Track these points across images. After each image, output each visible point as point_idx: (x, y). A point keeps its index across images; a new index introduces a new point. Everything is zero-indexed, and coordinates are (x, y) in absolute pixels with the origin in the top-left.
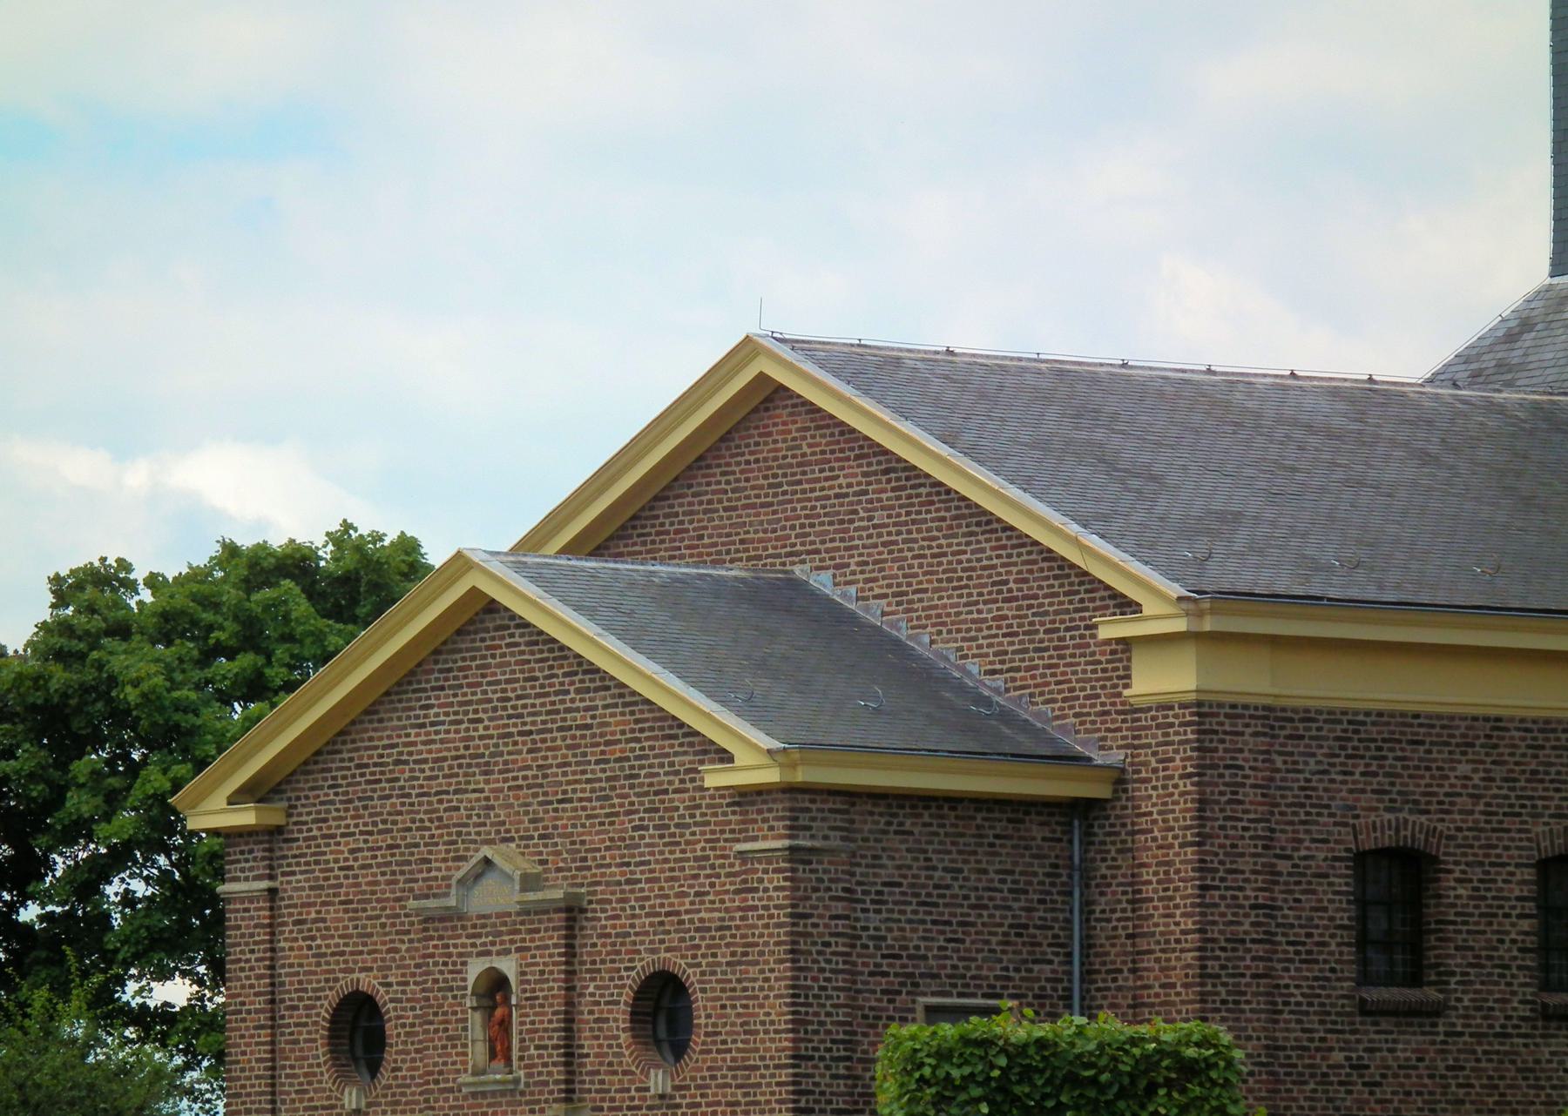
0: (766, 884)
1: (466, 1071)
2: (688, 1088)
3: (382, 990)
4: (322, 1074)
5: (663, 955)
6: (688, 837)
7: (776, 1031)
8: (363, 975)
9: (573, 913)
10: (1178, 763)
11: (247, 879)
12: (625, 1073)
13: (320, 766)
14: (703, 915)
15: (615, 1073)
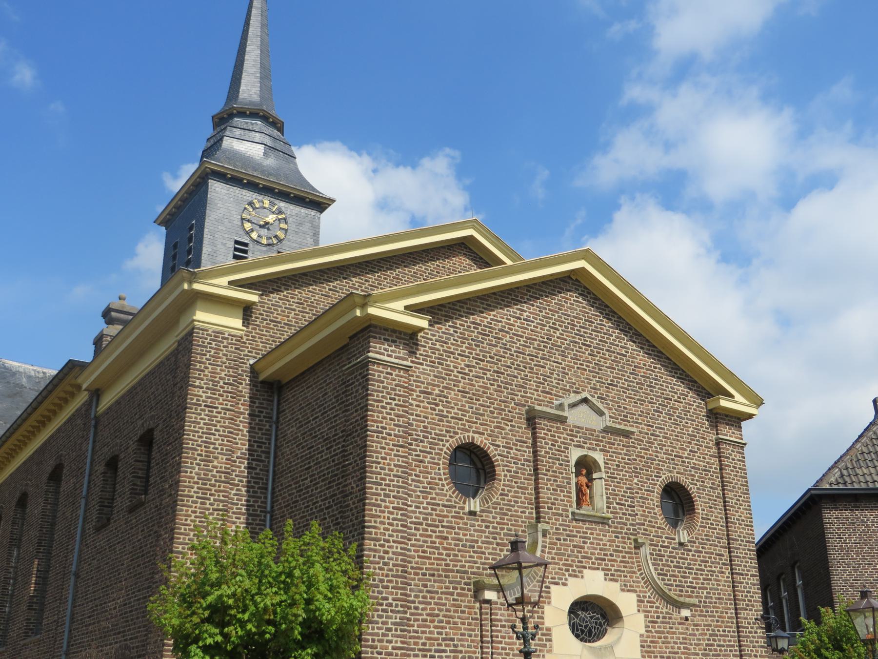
2: (695, 542)
3: (492, 448)
4: (443, 485)
7: (745, 525)
8: (476, 436)
12: (659, 528)
13: (443, 313)
15: (654, 527)
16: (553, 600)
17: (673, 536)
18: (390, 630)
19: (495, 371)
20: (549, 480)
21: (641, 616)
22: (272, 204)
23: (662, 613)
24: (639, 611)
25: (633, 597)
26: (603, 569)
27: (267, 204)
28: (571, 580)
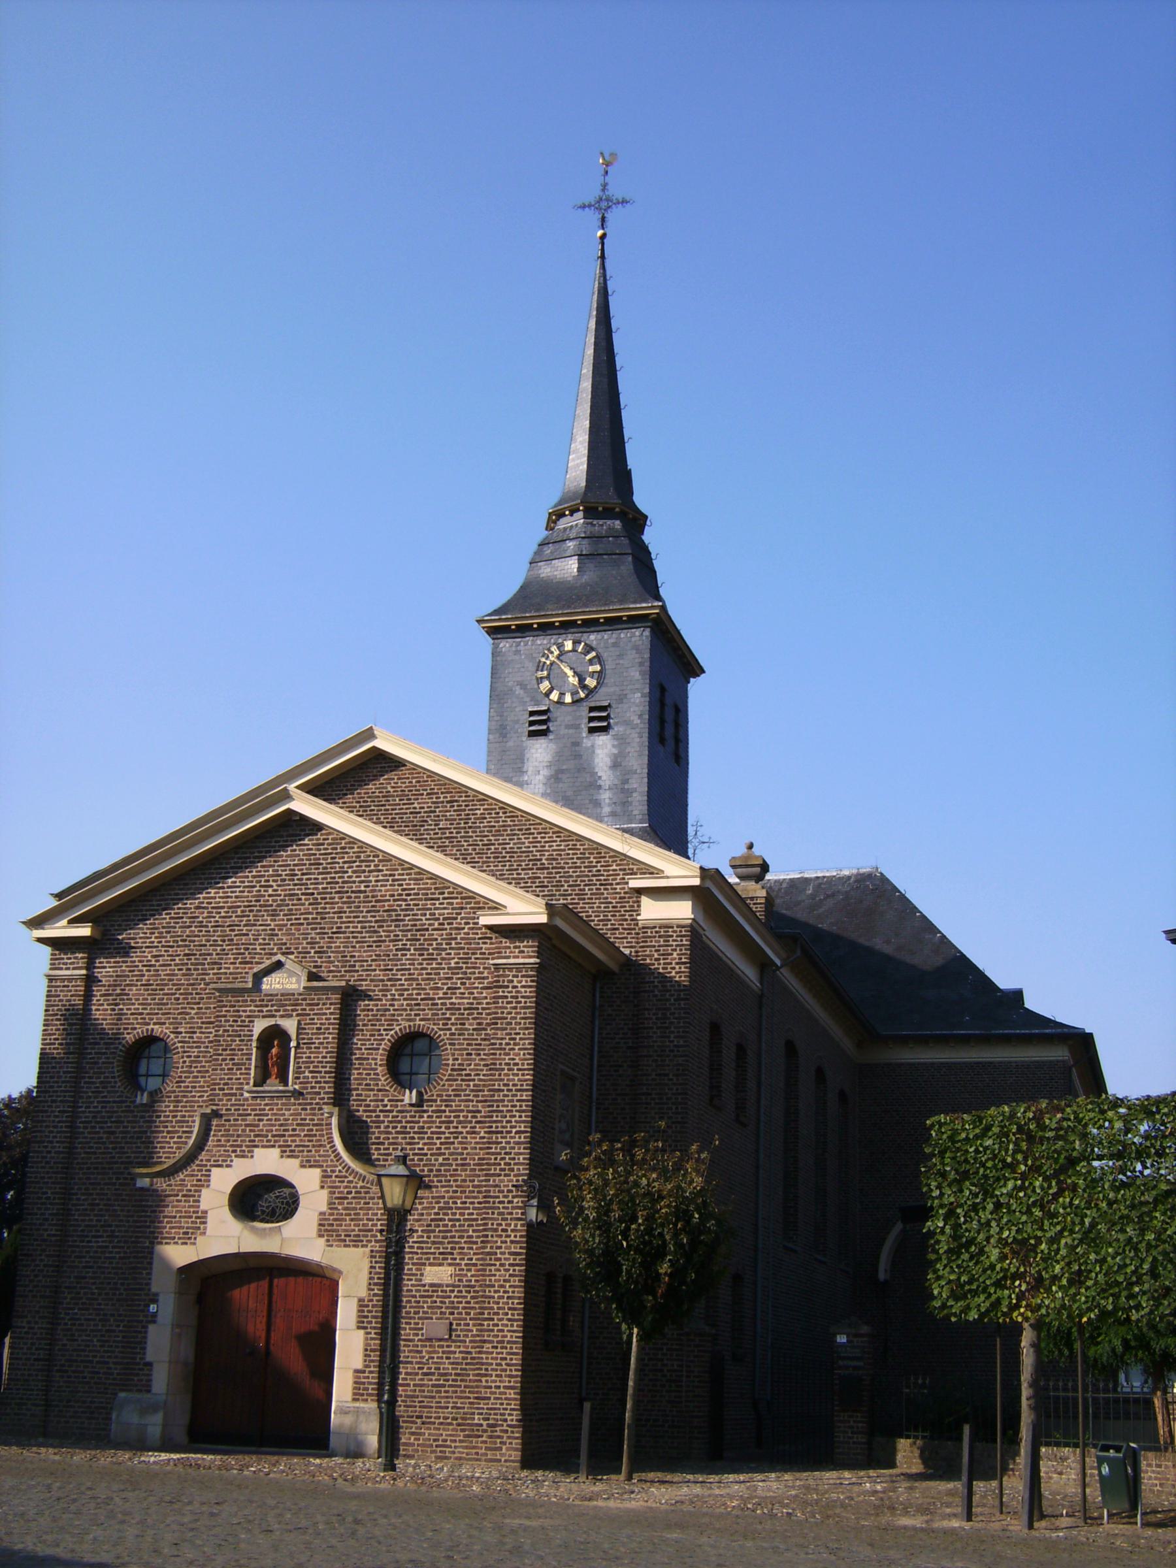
0: (515, 984)
1: (248, 1084)
3: (172, 1036)
5: (418, 1023)
6: (444, 955)
9: (350, 997)
10: (675, 955)
11: (68, 969)
14: (453, 1000)
16: (212, 1183)
17: (401, 1098)
18: (47, 1220)
19: (185, 955)
20: (224, 1060)
21: (325, 1192)
22: (576, 642)
23: (355, 1187)
24: (322, 1187)
25: (316, 1173)
26: (280, 1146)
27: (569, 645)
28: (237, 1162)
